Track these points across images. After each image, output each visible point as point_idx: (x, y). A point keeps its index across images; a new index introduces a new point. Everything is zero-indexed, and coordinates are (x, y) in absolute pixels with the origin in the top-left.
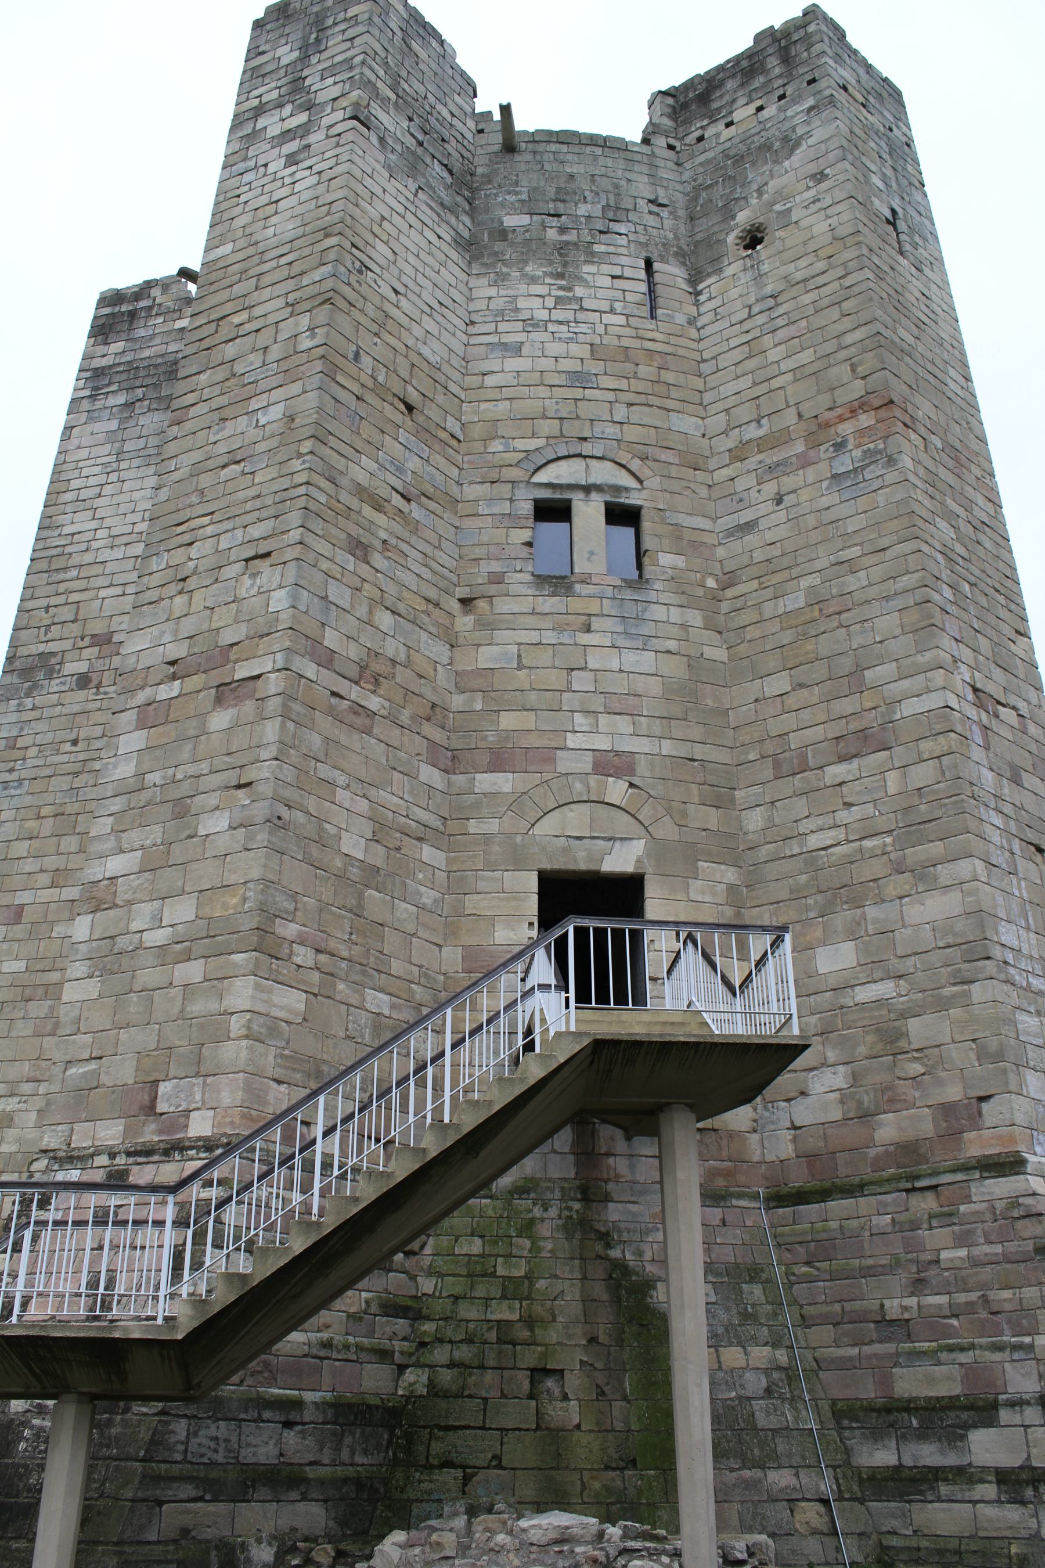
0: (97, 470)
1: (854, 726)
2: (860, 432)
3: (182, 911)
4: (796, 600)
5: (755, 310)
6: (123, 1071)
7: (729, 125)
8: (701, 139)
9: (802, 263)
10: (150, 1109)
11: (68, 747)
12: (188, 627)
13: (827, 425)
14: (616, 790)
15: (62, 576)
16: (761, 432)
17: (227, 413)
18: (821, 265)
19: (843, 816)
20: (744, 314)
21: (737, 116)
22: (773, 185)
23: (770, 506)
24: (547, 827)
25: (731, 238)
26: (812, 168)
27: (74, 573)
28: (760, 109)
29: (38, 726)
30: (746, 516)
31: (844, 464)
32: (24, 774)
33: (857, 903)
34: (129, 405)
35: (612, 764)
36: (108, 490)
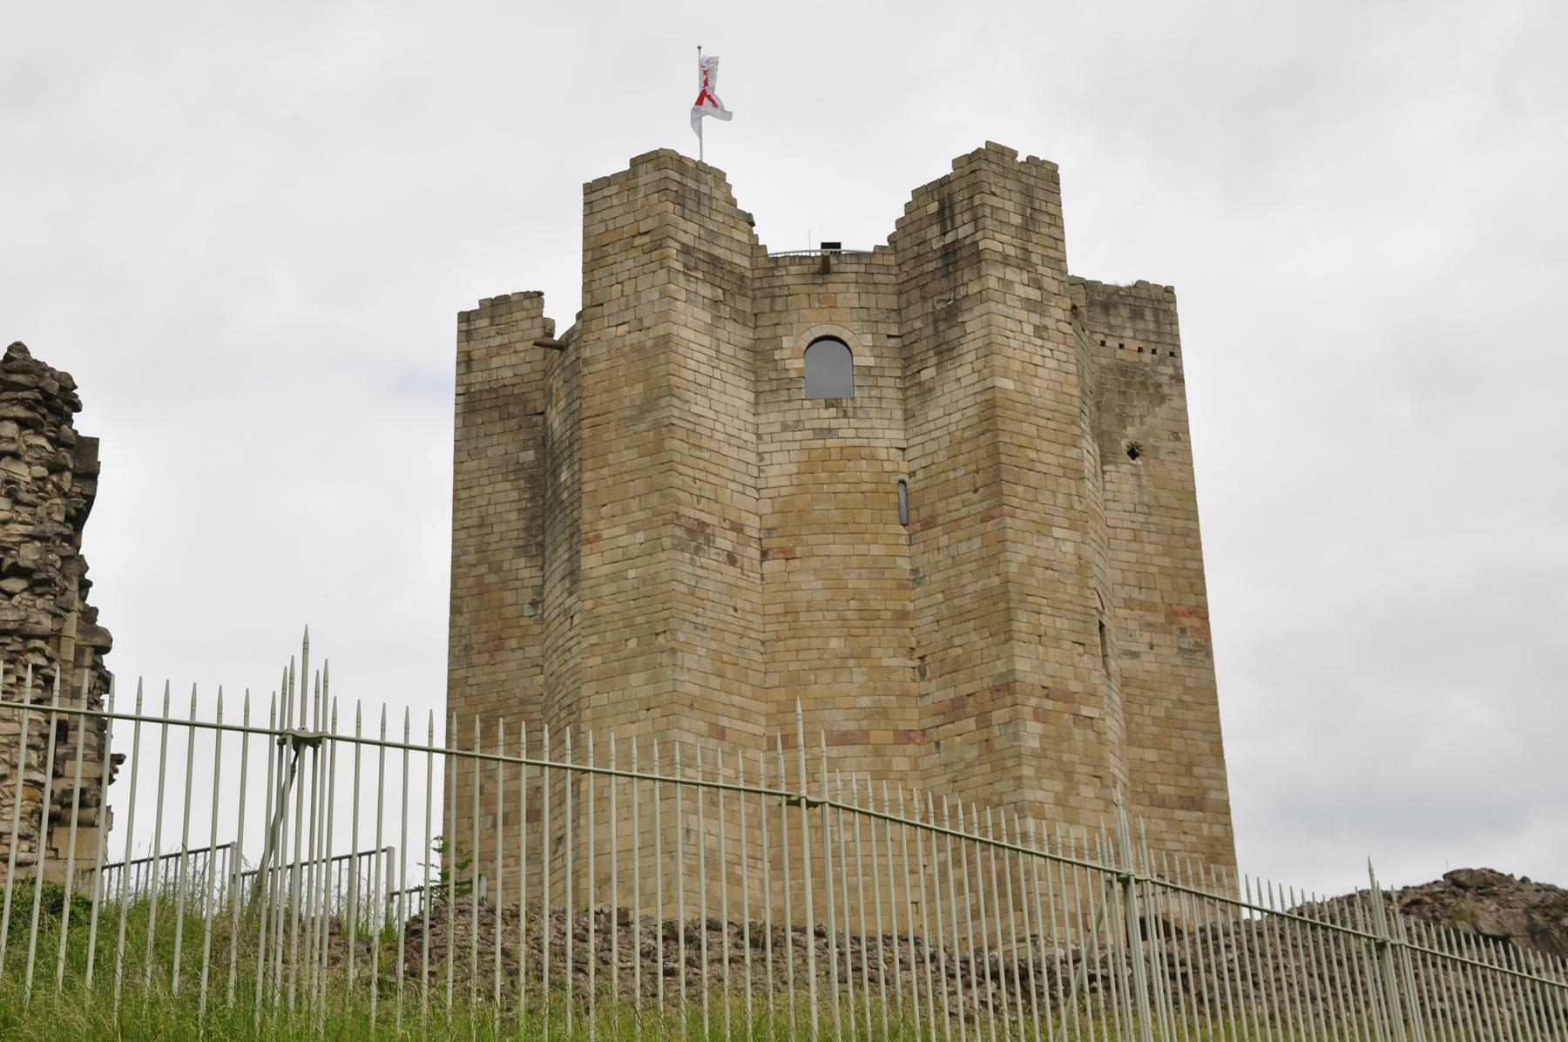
0: (704, 359)
1: (1188, 793)
5: (1139, 509)
11: (731, 611)
12: (1051, 668)
13: (1176, 614)
15: (697, 453)
16: (1142, 597)
17: (1041, 528)
18: (1175, 504)
19: (1182, 837)
20: (1131, 507)
22: (1148, 420)
23: (1145, 648)
25: (1124, 443)
27: (706, 455)
30: (1134, 647)
31: (1187, 642)
32: (706, 622)
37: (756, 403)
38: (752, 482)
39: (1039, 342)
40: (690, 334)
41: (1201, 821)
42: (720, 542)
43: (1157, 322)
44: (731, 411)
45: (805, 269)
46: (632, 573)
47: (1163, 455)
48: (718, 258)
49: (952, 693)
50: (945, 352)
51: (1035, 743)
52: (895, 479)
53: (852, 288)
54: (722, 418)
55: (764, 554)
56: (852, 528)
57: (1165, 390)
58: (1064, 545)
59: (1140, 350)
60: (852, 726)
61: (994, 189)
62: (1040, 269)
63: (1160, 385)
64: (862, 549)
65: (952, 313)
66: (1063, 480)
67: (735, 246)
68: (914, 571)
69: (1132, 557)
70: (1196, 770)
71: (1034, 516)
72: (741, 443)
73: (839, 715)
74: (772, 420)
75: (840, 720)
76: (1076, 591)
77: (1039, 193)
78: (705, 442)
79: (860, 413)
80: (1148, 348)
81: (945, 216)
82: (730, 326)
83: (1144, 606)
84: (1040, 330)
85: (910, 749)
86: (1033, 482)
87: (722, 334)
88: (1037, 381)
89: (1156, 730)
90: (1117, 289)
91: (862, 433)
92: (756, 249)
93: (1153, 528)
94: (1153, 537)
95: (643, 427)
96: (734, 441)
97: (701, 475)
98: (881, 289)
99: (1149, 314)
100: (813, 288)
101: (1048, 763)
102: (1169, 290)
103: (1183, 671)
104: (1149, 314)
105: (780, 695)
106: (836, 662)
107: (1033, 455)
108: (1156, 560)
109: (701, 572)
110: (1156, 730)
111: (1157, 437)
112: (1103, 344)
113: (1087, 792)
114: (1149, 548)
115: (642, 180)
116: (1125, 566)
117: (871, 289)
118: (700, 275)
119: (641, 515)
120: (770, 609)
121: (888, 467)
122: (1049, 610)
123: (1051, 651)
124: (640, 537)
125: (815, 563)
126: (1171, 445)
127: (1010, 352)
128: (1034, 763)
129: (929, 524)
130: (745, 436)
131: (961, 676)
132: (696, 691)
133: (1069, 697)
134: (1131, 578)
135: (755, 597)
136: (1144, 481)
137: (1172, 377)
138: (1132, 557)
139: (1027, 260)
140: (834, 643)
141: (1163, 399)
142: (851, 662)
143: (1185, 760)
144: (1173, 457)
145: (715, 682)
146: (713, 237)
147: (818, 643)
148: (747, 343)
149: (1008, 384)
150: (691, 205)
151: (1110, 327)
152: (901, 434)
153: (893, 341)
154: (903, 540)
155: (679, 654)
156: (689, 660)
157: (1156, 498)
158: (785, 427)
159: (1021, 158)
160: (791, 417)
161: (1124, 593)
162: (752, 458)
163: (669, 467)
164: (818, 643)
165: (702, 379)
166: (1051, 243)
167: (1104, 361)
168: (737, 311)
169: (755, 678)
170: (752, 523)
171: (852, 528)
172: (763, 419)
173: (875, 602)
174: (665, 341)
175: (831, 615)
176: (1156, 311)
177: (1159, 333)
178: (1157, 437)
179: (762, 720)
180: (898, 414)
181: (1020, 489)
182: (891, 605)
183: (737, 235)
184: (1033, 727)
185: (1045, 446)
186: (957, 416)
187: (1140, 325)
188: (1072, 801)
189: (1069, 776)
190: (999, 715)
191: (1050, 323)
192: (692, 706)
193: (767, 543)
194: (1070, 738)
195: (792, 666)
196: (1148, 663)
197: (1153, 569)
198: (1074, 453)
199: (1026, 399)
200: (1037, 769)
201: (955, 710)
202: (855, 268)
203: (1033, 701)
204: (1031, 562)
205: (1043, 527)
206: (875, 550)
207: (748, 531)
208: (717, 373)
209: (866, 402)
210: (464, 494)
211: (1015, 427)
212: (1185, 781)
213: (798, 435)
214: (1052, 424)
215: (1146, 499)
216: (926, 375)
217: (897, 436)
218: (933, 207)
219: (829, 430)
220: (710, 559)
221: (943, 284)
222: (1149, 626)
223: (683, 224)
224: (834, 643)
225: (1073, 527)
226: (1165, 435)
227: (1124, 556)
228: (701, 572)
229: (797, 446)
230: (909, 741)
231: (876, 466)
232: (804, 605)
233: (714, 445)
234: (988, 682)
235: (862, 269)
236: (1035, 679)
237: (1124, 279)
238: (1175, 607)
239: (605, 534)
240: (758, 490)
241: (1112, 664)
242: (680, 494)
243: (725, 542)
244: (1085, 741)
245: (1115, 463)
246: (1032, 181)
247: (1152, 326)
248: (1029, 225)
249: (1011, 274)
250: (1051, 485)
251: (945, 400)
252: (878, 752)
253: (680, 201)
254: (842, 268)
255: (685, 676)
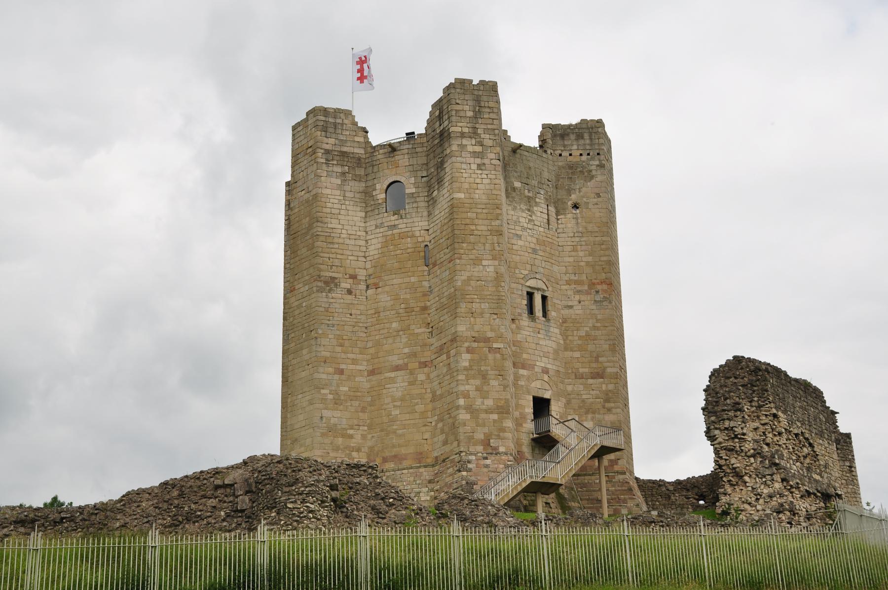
0: (336, 201)
2: (603, 290)
3: (489, 403)
4: (582, 333)
6: (480, 436)
7: (570, 155)
8: (560, 155)
9: (591, 225)
10: (489, 444)
11: (348, 316)
12: (476, 328)
13: (594, 284)
14: (546, 378)
15: (331, 246)
18: (596, 229)
19: (591, 392)
20: (572, 235)
21: (574, 153)
22: (584, 189)
23: (577, 303)
24: (533, 385)
25: (570, 203)
26: (597, 191)
27: (337, 246)
28: (581, 155)
29: (337, 306)
30: (570, 304)
31: (598, 298)
32: (334, 322)
33: (594, 413)
34: (343, 174)
35: (545, 371)
36: (342, 212)
37: (366, 217)
38: (363, 254)
39: (480, 172)
40: (328, 191)
41: (601, 383)
42: (343, 285)
43: (591, 139)
44: (351, 223)
45: (386, 150)
46: (304, 304)
47: (590, 206)
48: (346, 152)
49: (440, 343)
50: (440, 181)
51: (467, 364)
52: (423, 245)
53: (406, 156)
54: (346, 227)
55: (368, 287)
56: (403, 270)
57: (594, 173)
58: (489, 267)
59: (581, 155)
60: (401, 362)
61: (458, 101)
62: (482, 136)
63: (591, 171)
64: (407, 280)
65: (442, 163)
66: (489, 237)
67: (356, 145)
68: (430, 287)
69: (571, 259)
70: (600, 359)
71: (472, 257)
72: (357, 237)
73: (395, 358)
74: (372, 223)
75: (395, 360)
76: (494, 289)
77: (485, 98)
78: (336, 240)
79: (408, 216)
80: (585, 153)
81: (440, 117)
82: (352, 183)
83: (577, 282)
84: (480, 167)
85: (426, 370)
86: (472, 240)
87: (347, 188)
88: (477, 191)
89: (580, 342)
90: (570, 125)
91: (408, 225)
92: (368, 142)
93: (583, 243)
94: (583, 248)
95: (308, 237)
96: (353, 237)
97: (334, 256)
98: (419, 155)
99: (586, 136)
100: (390, 159)
101: (473, 372)
102: (600, 123)
103: (596, 312)
104: (586, 136)
105: (372, 351)
106: (395, 334)
107: (473, 227)
108: (584, 259)
109: (332, 300)
110: (580, 342)
111: (588, 198)
112: (560, 155)
113: (494, 383)
114: (581, 254)
115: (310, 122)
116: (567, 264)
117: (415, 155)
118: (335, 162)
119: (307, 278)
120: (370, 312)
121: (420, 239)
122: (478, 301)
123: (478, 320)
124: (307, 287)
125: (387, 289)
126: (595, 200)
127: (463, 180)
128: (465, 373)
129: (435, 265)
130: (359, 233)
131: (442, 335)
132: (328, 354)
133: (487, 340)
134: (570, 269)
135: (362, 307)
136: (579, 221)
137: (598, 166)
138: (571, 259)
139: (475, 133)
140: (394, 325)
141: (592, 177)
142: (401, 333)
143: (595, 355)
144: (596, 206)
145: (339, 349)
146: (343, 143)
147: (387, 325)
148: (361, 189)
149: (462, 196)
150: (331, 130)
151: (565, 146)
152: (426, 223)
153: (424, 179)
154: (426, 273)
155: (319, 340)
156: (324, 341)
157: (586, 228)
158: (377, 227)
159: (475, 82)
160: (379, 221)
161: (566, 278)
162: (363, 243)
163: (316, 255)
164: (387, 325)
165: (334, 211)
166: (490, 121)
167: (560, 164)
168: (356, 175)
169: (360, 344)
170: (362, 274)
171: (403, 270)
172: (368, 224)
173: (412, 304)
174: (316, 196)
175: (393, 312)
176: (590, 134)
177: (591, 145)
178: (588, 198)
179: (365, 363)
180: (425, 214)
181: (464, 245)
182: (420, 304)
183: (357, 139)
184: (466, 356)
185: (480, 222)
186: (443, 213)
187: (581, 142)
188: (485, 388)
189: (484, 377)
190: (453, 352)
191: (486, 161)
192: (325, 362)
193: (369, 282)
194: (486, 358)
195: (377, 337)
196: (578, 310)
197: (582, 264)
198: (497, 222)
199: (471, 201)
200: (467, 376)
201: (440, 350)
202: (407, 146)
203: (466, 344)
204: (469, 279)
205: (477, 261)
206: (413, 279)
207: (359, 277)
208: (344, 207)
209: (411, 210)
210: (288, 266)
211: (464, 215)
212: (594, 365)
213: (382, 230)
214: (484, 211)
215: (580, 229)
216: (435, 193)
217: (424, 224)
218: (437, 113)
219: (394, 225)
220: (337, 294)
221: (439, 150)
222: (579, 292)
223: (326, 140)
224: (394, 325)
225: (494, 259)
226: (593, 195)
227: (567, 259)
228: (332, 300)
229: (381, 235)
230: (426, 366)
231: (415, 240)
232: (382, 309)
233: (341, 241)
234: (450, 337)
235: (411, 146)
236: (469, 334)
237: (575, 121)
238: (594, 281)
239: (297, 287)
240: (365, 257)
241: (552, 314)
242: (321, 266)
243: (346, 285)
244: (495, 359)
245: (565, 214)
246: (481, 93)
247: (588, 142)
248: (477, 114)
249: (465, 141)
250: (483, 240)
251: (439, 206)
252: (411, 373)
253: (325, 129)
254: (402, 147)
255: (322, 349)
